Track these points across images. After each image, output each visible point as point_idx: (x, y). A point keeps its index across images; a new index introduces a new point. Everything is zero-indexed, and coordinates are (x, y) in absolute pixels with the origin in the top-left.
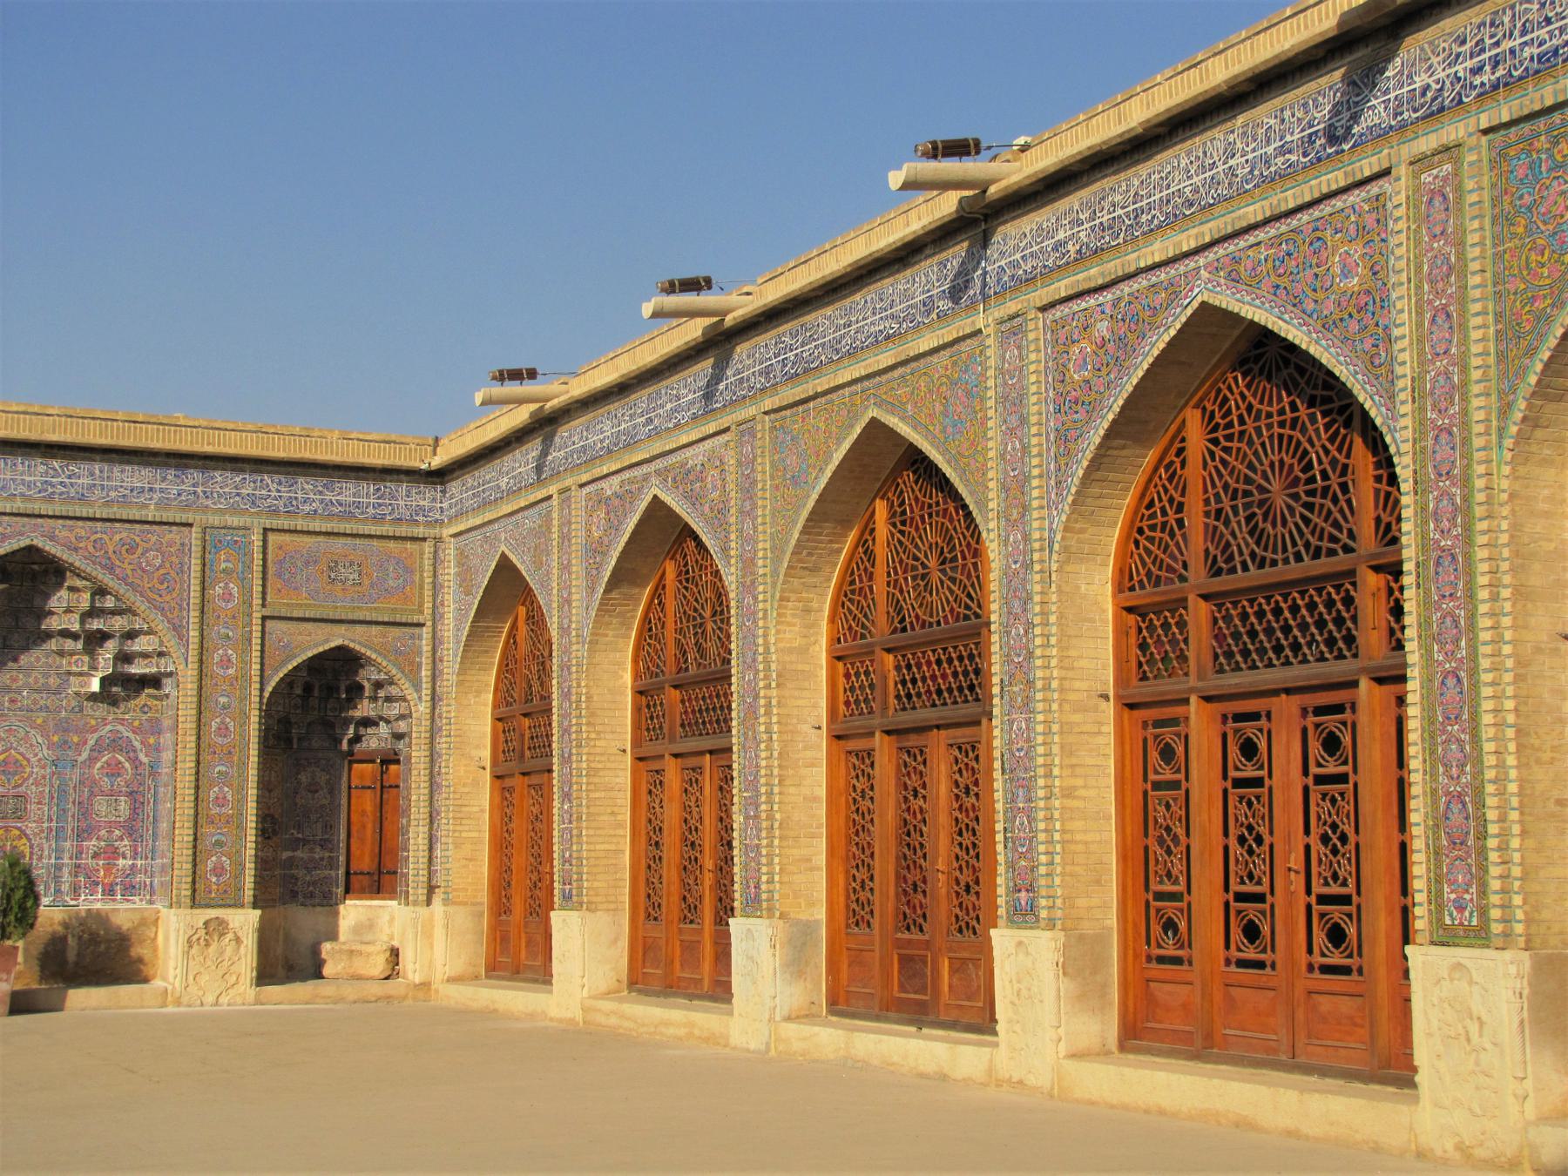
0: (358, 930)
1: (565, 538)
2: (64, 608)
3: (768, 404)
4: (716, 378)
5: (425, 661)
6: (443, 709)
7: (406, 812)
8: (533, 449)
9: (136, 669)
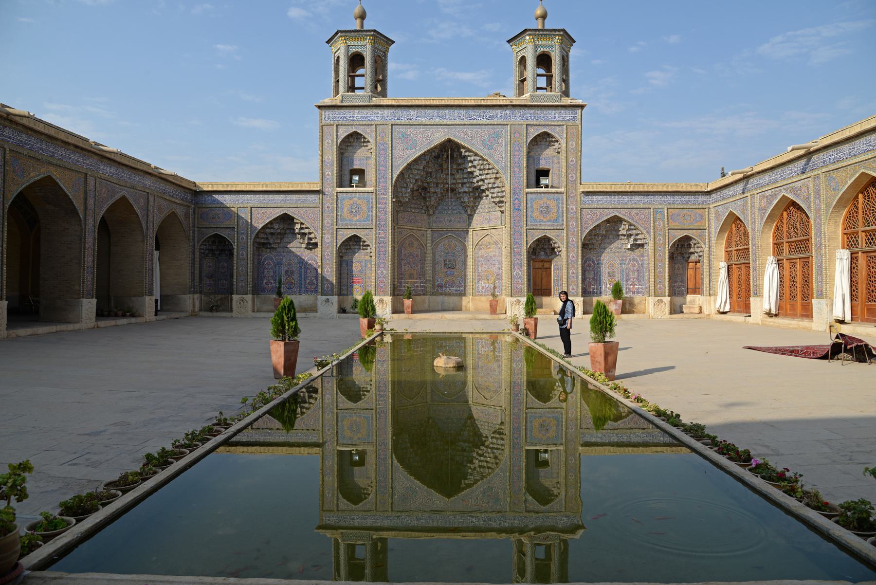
0: (690, 302)
1: (753, 207)
2: (623, 229)
3: (824, 170)
4: (807, 164)
5: (707, 237)
6: (712, 249)
7: (703, 274)
8: (741, 186)
9: (639, 242)
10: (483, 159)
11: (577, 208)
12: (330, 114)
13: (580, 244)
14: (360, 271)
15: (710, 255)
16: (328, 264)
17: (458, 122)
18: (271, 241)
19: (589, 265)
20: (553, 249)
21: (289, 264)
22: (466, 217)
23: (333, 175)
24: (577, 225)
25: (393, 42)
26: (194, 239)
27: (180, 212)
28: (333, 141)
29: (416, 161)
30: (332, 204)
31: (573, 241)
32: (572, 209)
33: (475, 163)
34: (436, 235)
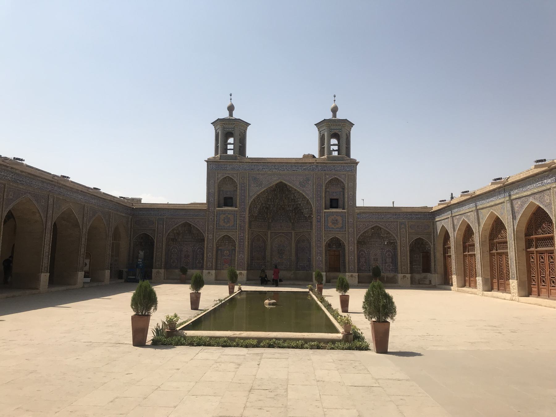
10: (298, 192)
13: (356, 242)
15: (434, 249)
19: (362, 254)
22: (291, 224)
26: (130, 236)
28: (215, 181)
30: (214, 217)
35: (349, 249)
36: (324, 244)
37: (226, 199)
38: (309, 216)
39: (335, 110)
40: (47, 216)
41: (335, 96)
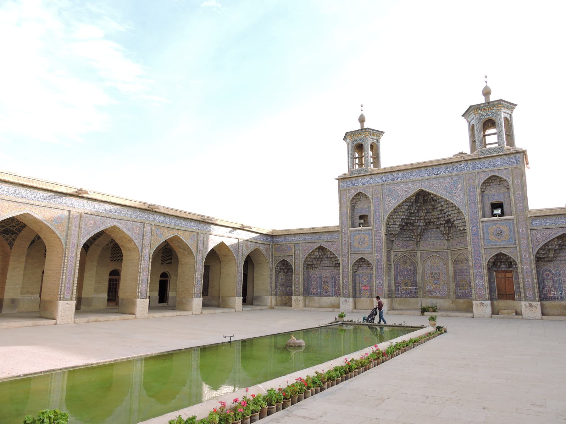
10: (446, 201)
11: (527, 230)
12: (345, 183)
13: (533, 258)
14: (367, 281)
16: (346, 277)
17: (426, 177)
18: (315, 263)
19: (548, 275)
20: (511, 262)
21: (326, 277)
22: (445, 242)
23: (347, 220)
24: (528, 243)
25: (383, 132)
27: (262, 248)
28: (347, 200)
29: (399, 206)
30: (348, 238)
31: (525, 256)
32: (523, 231)
33: (442, 204)
34: (424, 255)
35: (522, 269)
36: (485, 263)
37: (361, 217)
38: (464, 229)
39: (487, 93)
40: (142, 243)
41: (486, 77)
